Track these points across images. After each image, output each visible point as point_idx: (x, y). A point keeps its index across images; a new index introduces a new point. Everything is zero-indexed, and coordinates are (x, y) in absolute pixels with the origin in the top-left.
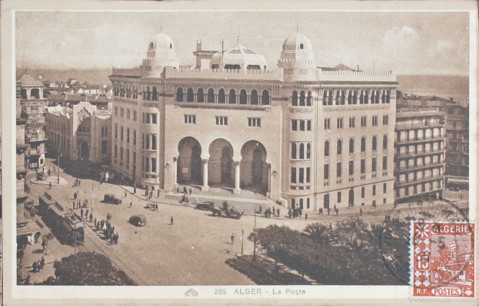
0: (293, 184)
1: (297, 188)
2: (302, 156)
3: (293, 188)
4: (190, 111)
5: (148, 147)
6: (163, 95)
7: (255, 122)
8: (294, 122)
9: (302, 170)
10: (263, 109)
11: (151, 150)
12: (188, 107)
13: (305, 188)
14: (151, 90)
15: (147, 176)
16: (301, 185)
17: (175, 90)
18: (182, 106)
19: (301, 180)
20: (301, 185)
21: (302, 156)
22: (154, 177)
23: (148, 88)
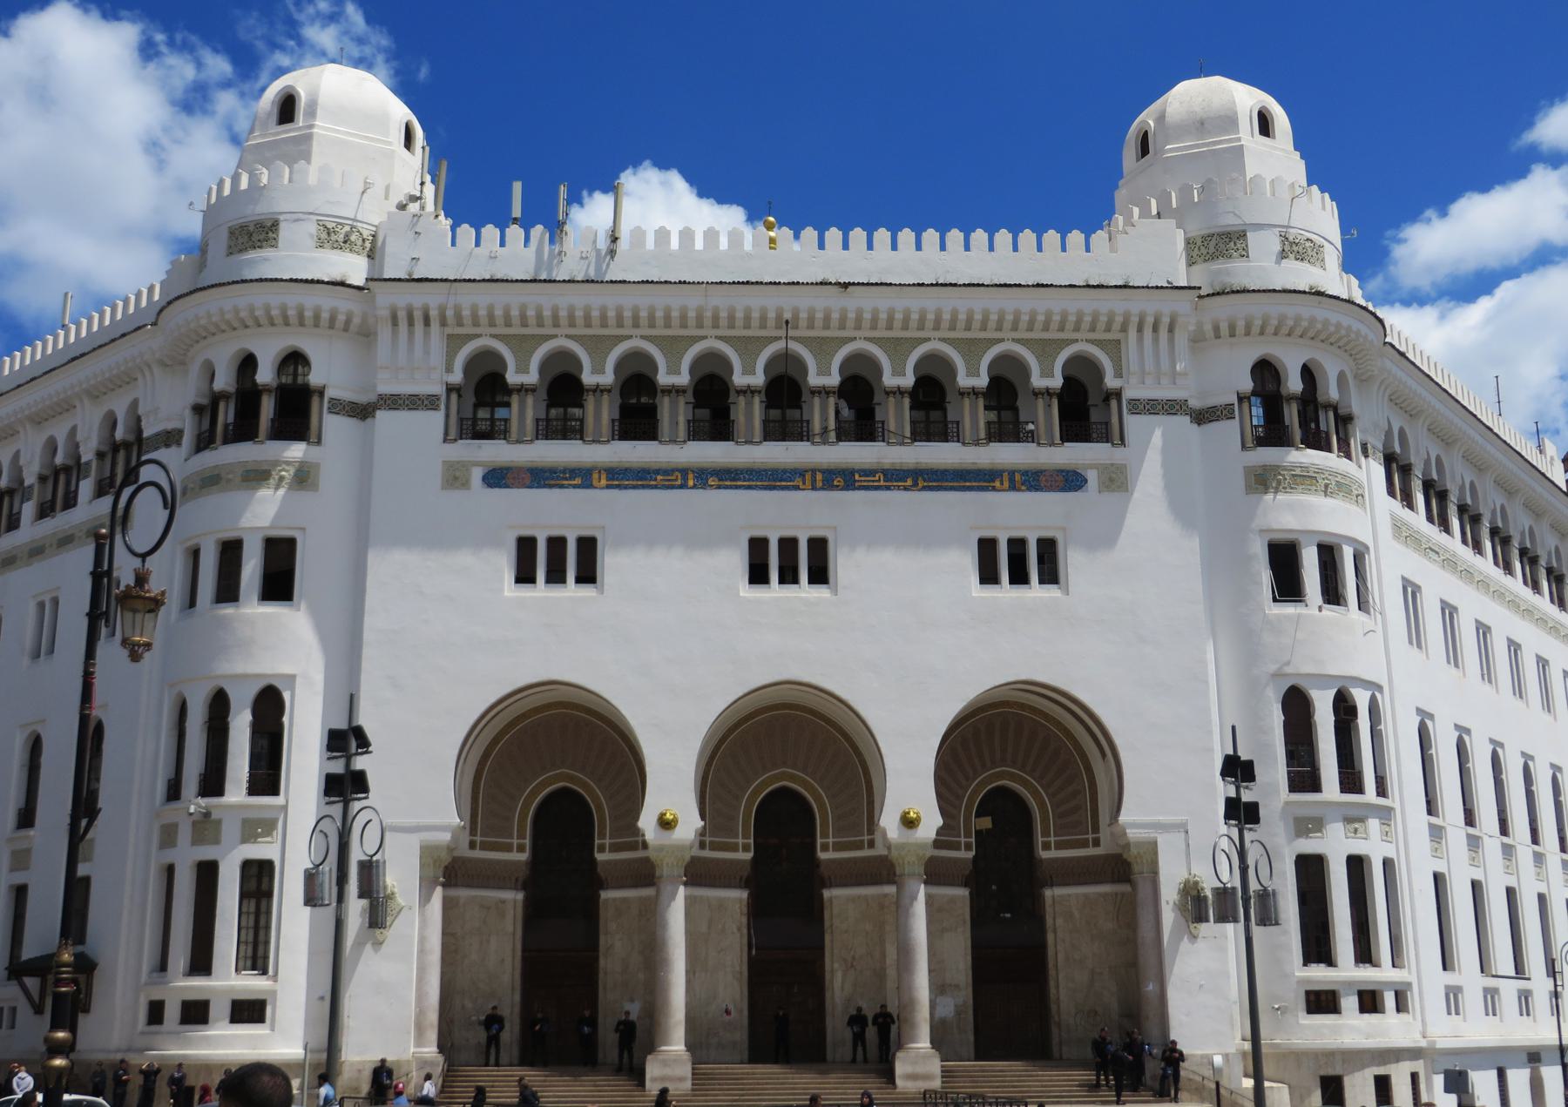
0: (1319, 974)
1: (1350, 1003)
2: (1350, 782)
3: (1322, 1002)
4: (557, 513)
5: (213, 783)
6: (362, 412)
7: (1017, 562)
8: (1284, 559)
9: (1357, 865)
10: (1071, 480)
11: (236, 790)
12: (542, 477)
13: (1389, 1000)
14: (265, 375)
15: (196, 1013)
16: (1366, 974)
17: (449, 369)
18: (497, 477)
19: (1365, 954)
20: (1366, 974)
21: (1350, 782)
22: (249, 1011)
23: (248, 363)
